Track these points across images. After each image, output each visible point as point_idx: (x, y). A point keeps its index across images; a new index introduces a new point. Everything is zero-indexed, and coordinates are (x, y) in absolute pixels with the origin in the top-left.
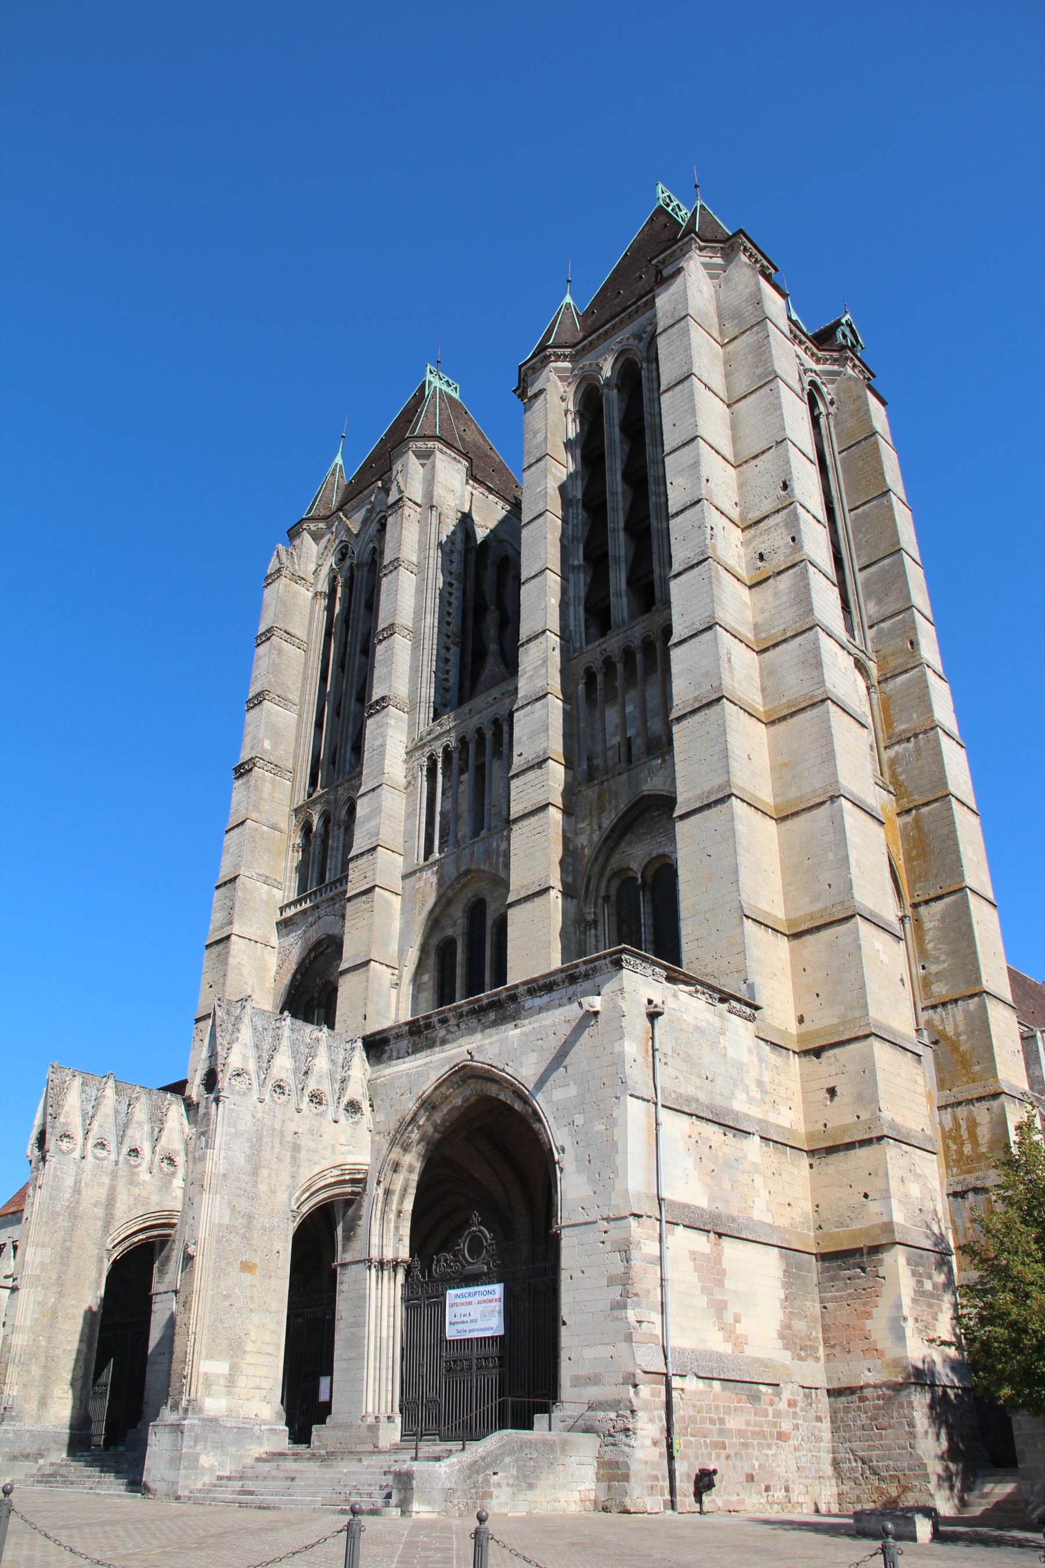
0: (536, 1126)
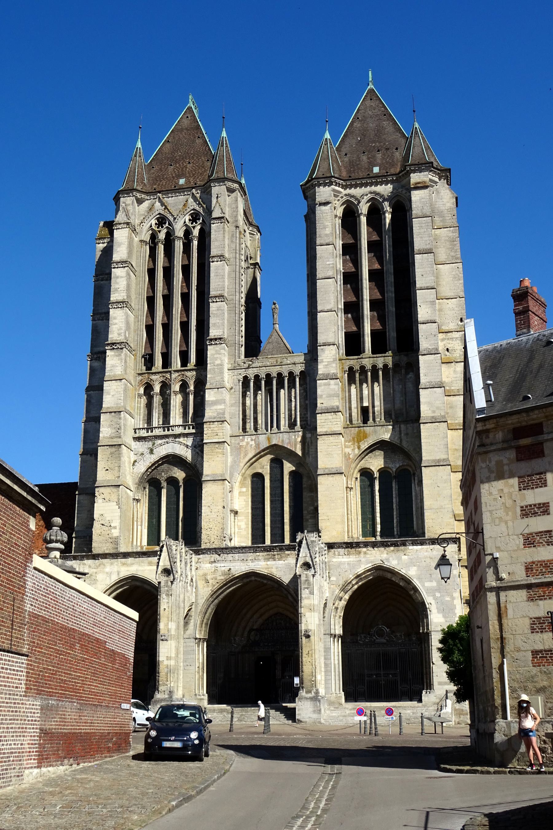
0: (412, 592)
